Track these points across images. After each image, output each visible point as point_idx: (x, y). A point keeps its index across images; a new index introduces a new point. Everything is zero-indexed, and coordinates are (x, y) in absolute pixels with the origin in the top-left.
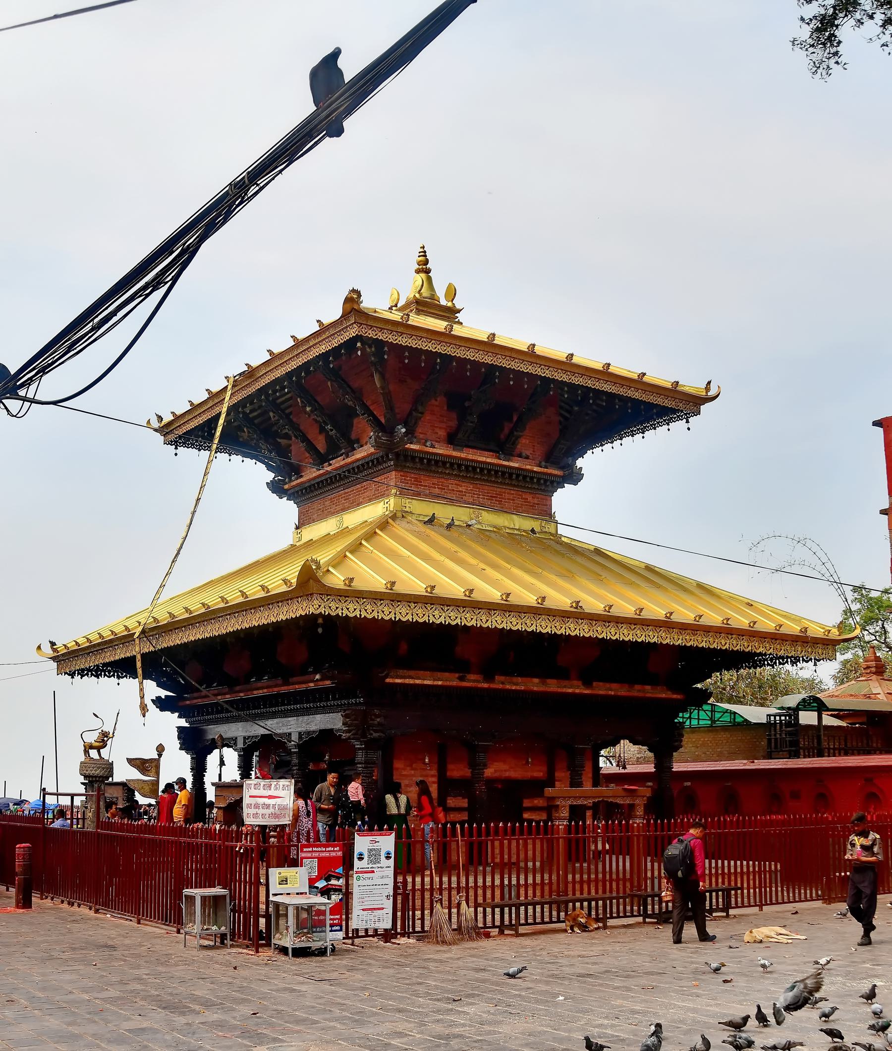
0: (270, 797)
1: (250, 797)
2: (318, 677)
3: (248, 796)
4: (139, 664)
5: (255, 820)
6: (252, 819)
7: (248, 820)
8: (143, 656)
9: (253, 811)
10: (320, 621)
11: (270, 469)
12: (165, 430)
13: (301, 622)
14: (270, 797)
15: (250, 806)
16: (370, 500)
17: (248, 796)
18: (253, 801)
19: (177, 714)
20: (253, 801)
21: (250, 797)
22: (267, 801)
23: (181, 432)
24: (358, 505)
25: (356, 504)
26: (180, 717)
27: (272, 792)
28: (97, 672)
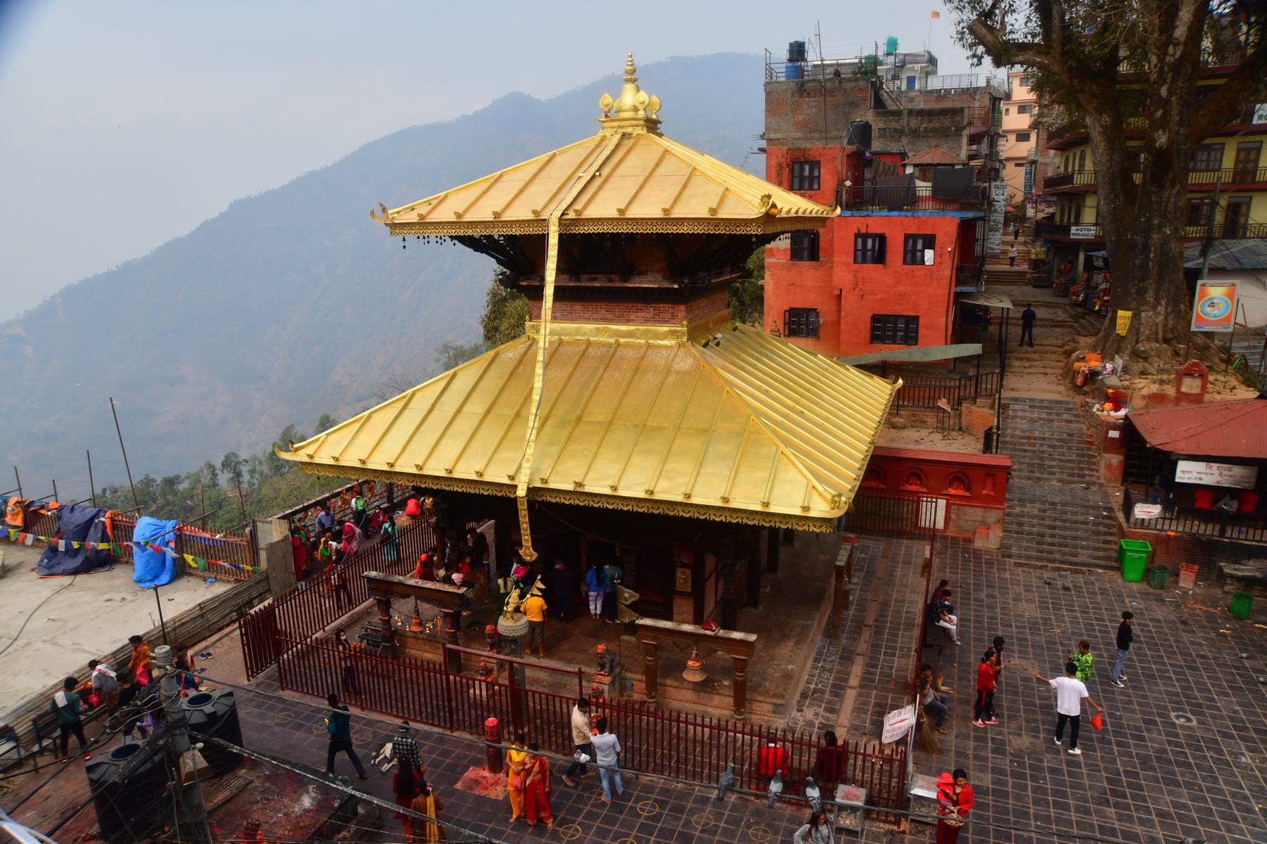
0: (902, 721)
11: (499, 262)
14: (902, 721)
20: (891, 727)
22: (899, 724)
25: (628, 321)
27: (902, 718)
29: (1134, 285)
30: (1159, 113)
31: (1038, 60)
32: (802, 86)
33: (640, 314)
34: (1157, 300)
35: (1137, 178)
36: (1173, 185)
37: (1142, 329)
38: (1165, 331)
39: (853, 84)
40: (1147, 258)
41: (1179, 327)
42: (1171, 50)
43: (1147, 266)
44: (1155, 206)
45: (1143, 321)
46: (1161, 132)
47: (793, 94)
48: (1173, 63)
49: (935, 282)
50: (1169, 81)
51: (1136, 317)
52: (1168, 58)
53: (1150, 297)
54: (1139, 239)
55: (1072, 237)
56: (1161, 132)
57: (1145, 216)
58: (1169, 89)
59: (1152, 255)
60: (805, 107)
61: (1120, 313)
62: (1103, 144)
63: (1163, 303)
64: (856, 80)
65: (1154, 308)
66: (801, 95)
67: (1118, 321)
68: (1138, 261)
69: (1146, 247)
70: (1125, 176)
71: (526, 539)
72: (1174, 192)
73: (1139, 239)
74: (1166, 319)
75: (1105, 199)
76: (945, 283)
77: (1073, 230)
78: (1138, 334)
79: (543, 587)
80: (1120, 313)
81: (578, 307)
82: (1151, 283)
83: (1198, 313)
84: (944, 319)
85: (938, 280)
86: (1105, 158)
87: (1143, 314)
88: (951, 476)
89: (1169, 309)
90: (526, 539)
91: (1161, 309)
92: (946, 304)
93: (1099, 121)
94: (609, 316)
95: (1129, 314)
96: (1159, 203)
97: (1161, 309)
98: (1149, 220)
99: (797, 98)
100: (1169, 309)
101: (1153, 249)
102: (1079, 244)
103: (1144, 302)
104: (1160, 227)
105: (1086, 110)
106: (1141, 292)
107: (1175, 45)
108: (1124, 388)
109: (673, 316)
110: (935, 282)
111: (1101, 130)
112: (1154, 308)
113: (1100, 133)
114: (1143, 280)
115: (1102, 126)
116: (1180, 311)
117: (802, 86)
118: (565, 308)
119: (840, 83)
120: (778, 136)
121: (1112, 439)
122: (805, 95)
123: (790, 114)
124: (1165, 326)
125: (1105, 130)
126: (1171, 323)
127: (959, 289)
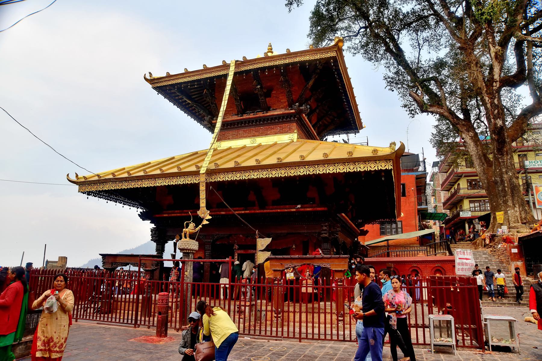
1: (460, 259)
2: (299, 206)
3: (457, 258)
5: (462, 272)
6: (461, 272)
7: (458, 272)
8: (208, 185)
9: (461, 267)
10: (383, 174)
12: (152, 81)
13: (297, 178)
15: (459, 264)
17: (457, 258)
18: (461, 261)
19: (150, 221)
20: (461, 261)
21: (460, 259)
23: (159, 85)
26: (151, 223)
28: (99, 194)
29: (501, 200)
30: (496, 111)
31: (439, 110)
33: (272, 131)
34: (514, 205)
35: (491, 156)
36: (507, 154)
37: (510, 219)
38: (521, 220)
40: (504, 187)
41: (528, 218)
42: (494, 84)
43: (505, 190)
44: (502, 164)
45: (510, 215)
46: (498, 120)
48: (497, 89)
49: (408, 204)
50: (497, 97)
51: (506, 213)
52: (494, 87)
53: (510, 203)
54: (498, 179)
55: (461, 216)
56: (498, 120)
57: (498, 168)
58: (498, 101)
59: (506, 185)
61: (497, 213)
62: (472, 143)
63: (517, 206)
65: (514, 209)
67: (497, 217)
68: (500, 189)
69: (502, 181)
70: (485, 156)
71: (203, 203)
72: (509, 157)
73: (498, 179)
74: (520, 214)
75: (478, 166)
76: (412, 204)
77: (461, 213)
78: (509, 222)
79: (210, 217)
80: (497, 213)
82: (509, 197)
83: (538, 200)
84: (414, 221)
85: (409, 203)
86: (475, 148)
87: (509, 212)
88: (434, 270)
89: (521, 209)
90: (203, 203)
91: (517, 209)
92: (414, 214)
93: (468, 135)
95: (502, 213)
96: (504, 162)
97: (517, 209)
98: (501, 170)
100: (521, 209)
101: (506, 182)
102: (465, 220)
103: (508, 206)
104: (507, 172)
105: (462, 132)
106: (505, 202)
107: (496, 82)
108: (512, 235)
109: (290, 129)
110: (408, 204)
111: (470, 138)
112: (514, 209)
113: (470, 139)
114: (505, 196)
115: (470, 136)
116: (526, 210)
118: (234, 133)
121: (514, 253)
124: (521, 217)
125: (472, 138)
126: (523, 216)
127: (419, 207)
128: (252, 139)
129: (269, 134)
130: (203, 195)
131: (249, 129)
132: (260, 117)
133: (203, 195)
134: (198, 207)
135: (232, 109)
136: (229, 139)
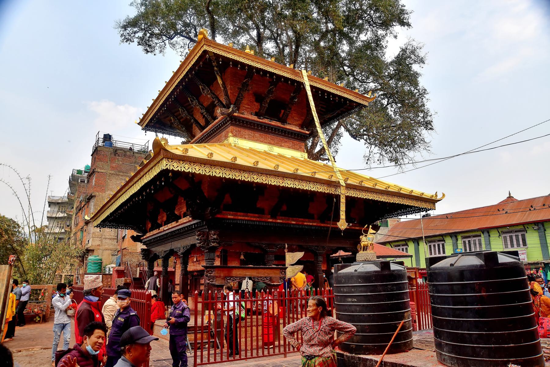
4: (343, 200)
16: (289, 148)
24: (281, 146)
32: (116, 151)
33: (286, 144)
39: (139, 155)
47: (111, 154)
60: (117, 160)
64: (141, 154)
66: (115, 155)
71: (343, 215)
81: (257, 134)
90: (343, 215)
94: (273, 142)
99: (113, 156)
109: (300, 148)
117: (116, 151)
118: (250, 134)
119: (133, 153)
120: (102, 171)
122: (117, 155)
123: (109, 162)
128: (270, 146)
129: (283, 146)
130: (343, 207)
131: (266, 135)
132: (265, 123)
133: (343, 207)
134: (338, 219)
135: (249, 107)
136: (245, 138)
